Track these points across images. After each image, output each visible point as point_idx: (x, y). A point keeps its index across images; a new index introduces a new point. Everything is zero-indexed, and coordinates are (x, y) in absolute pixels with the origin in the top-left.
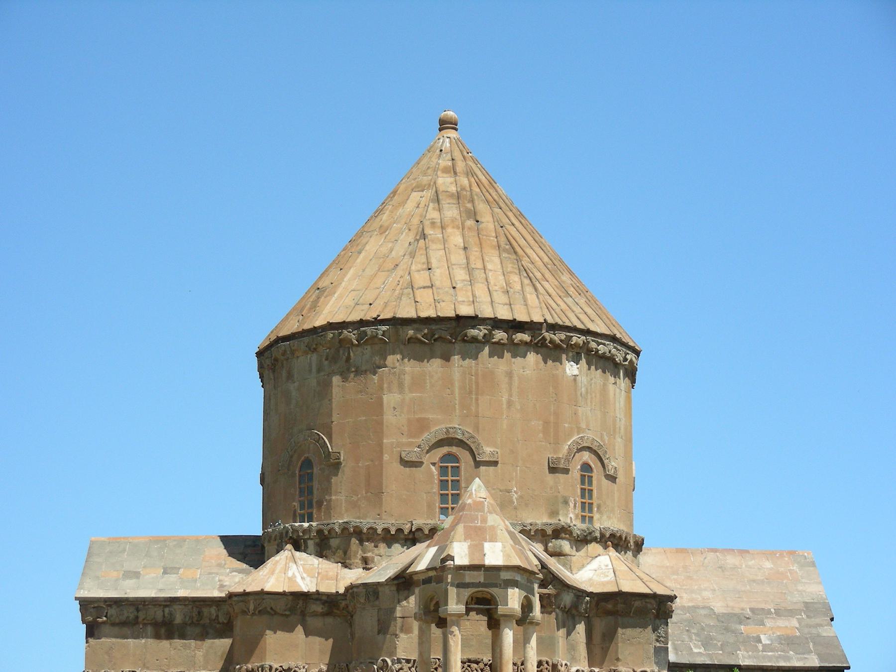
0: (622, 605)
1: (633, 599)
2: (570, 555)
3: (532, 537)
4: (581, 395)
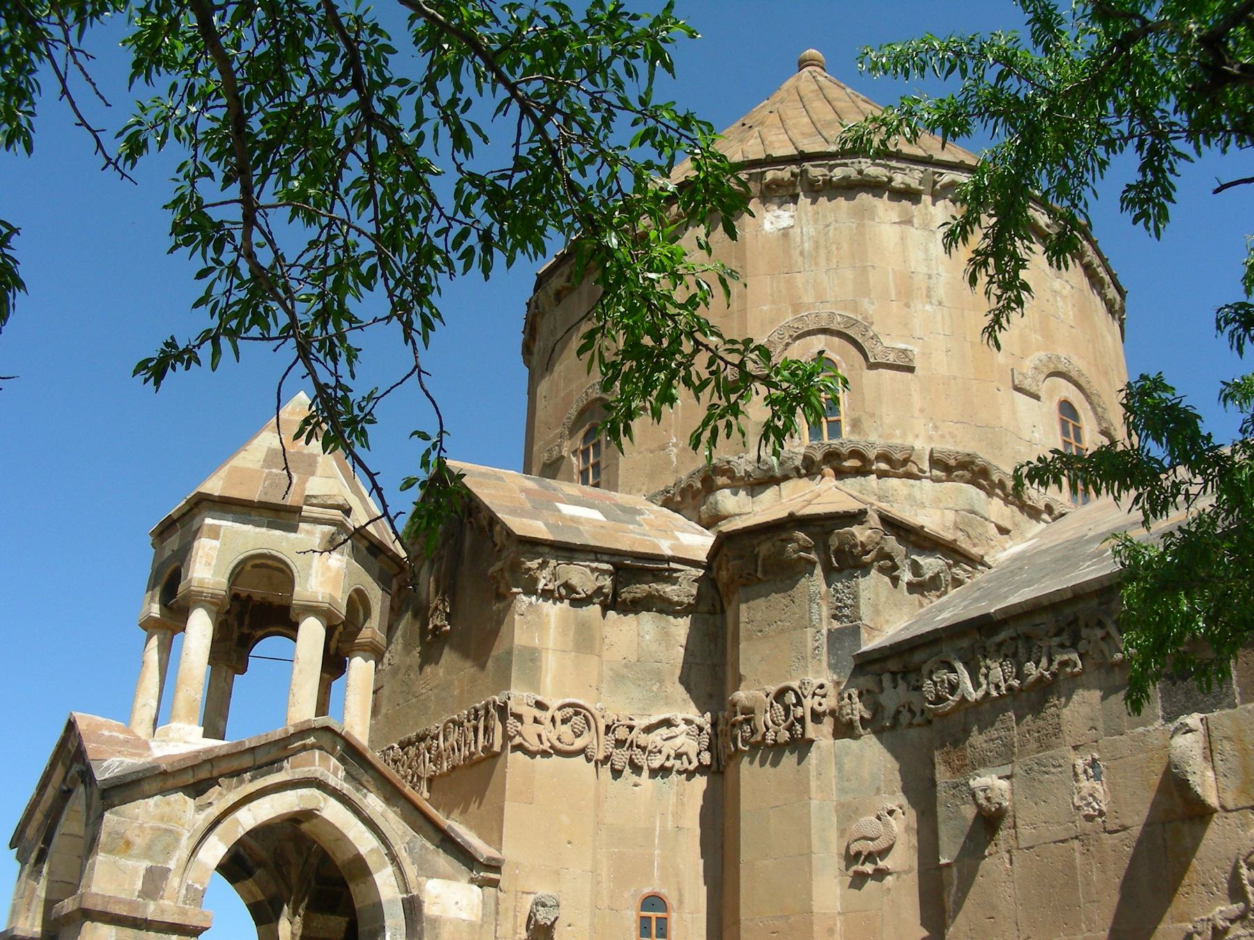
0: (736, 562)
1: (755, 542)
2: (739, 515)
3: (681, 507)
4: (802, 253)
